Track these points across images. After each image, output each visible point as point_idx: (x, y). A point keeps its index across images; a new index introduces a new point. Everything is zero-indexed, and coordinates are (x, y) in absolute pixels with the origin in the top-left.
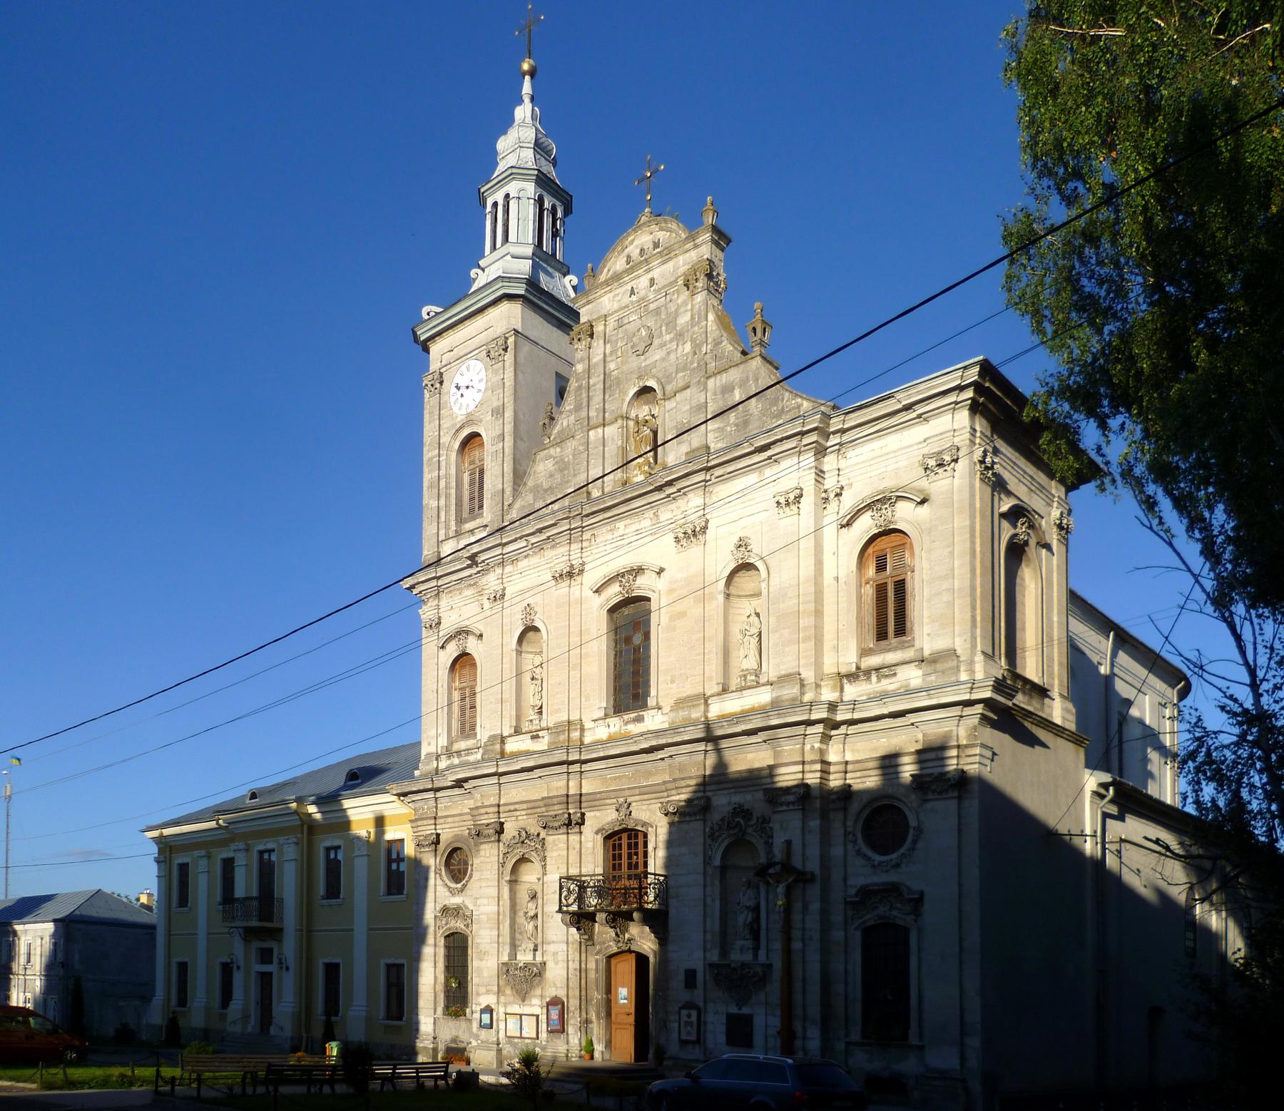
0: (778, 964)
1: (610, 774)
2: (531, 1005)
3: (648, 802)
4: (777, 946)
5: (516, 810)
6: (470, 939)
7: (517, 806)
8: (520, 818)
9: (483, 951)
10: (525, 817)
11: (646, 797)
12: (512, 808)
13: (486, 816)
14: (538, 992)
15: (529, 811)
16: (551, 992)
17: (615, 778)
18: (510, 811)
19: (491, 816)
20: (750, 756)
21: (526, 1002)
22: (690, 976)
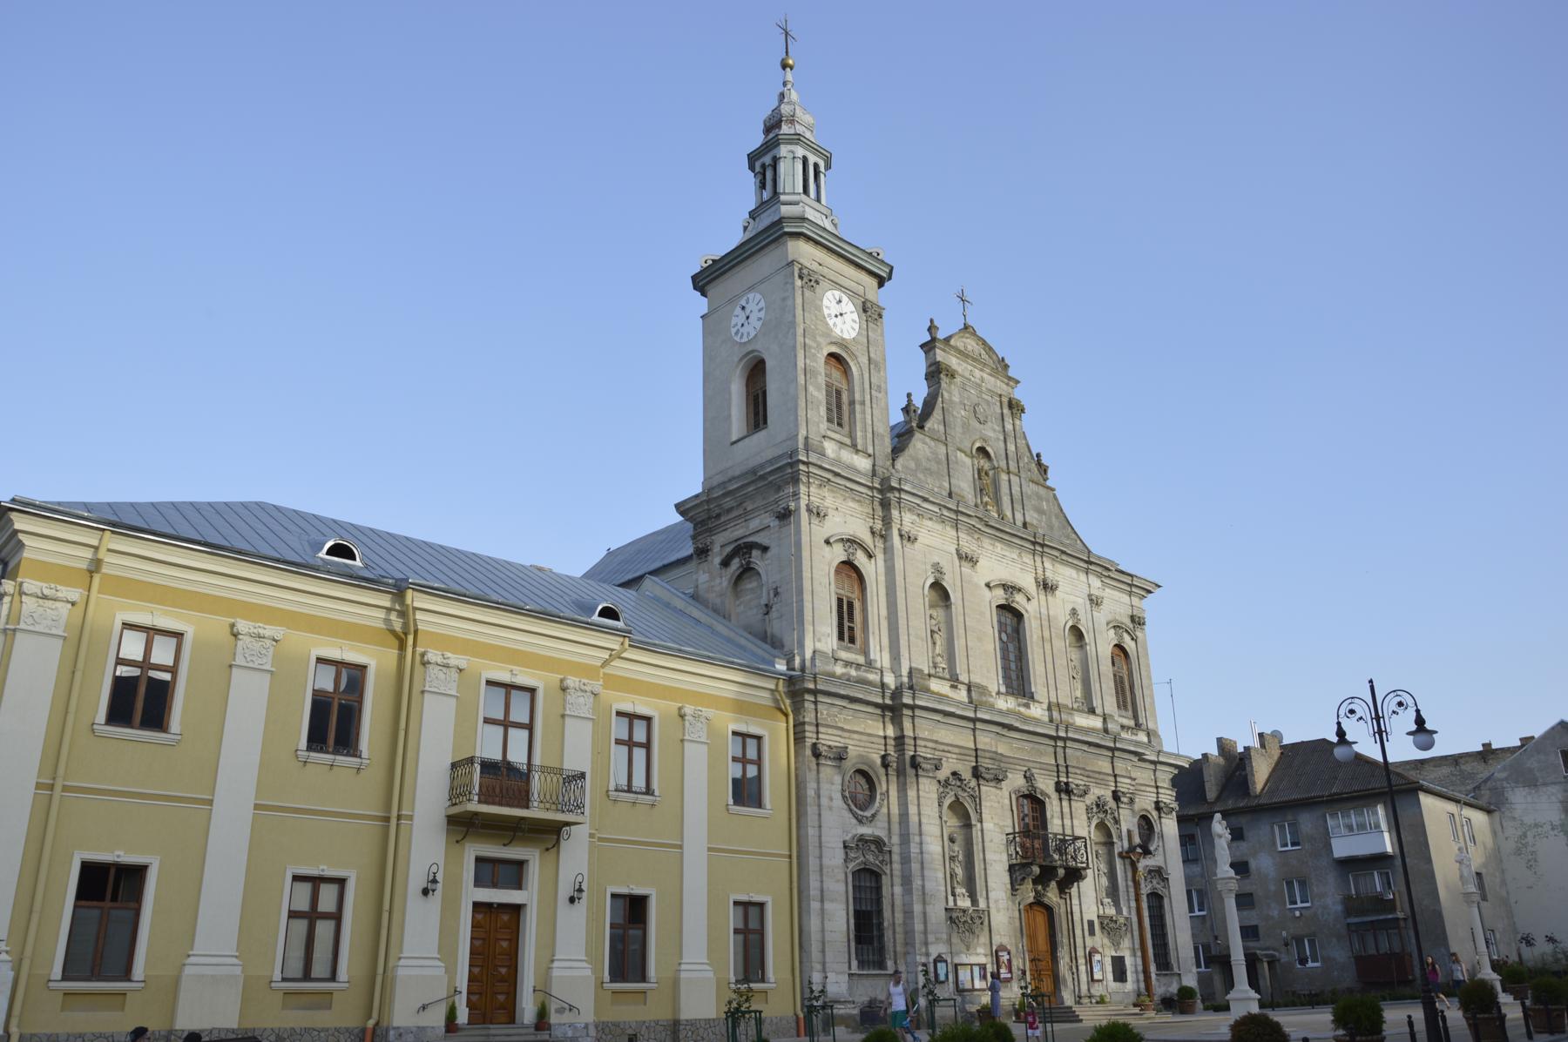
0: (1135, 919)
1: (1016, 744)
2: (978, 954)
3: (1043, 776)
4: (1133, 904)
5: (949, 752)
6: (885, 880)
7: (950, 748)
8: (951, 760)
9: (930, 894)
10: (955, 761)
11: (1042, 771)
12: (946, 748)
13: (924, 750)
14: (984, 939)
15: (960, 757)
16: (997, 940)
17: (1019, 749)
18: (943, 751)
19: (929, 750)
20: (1100, 763)
21: (971, 951)
22: (1091, 923)
